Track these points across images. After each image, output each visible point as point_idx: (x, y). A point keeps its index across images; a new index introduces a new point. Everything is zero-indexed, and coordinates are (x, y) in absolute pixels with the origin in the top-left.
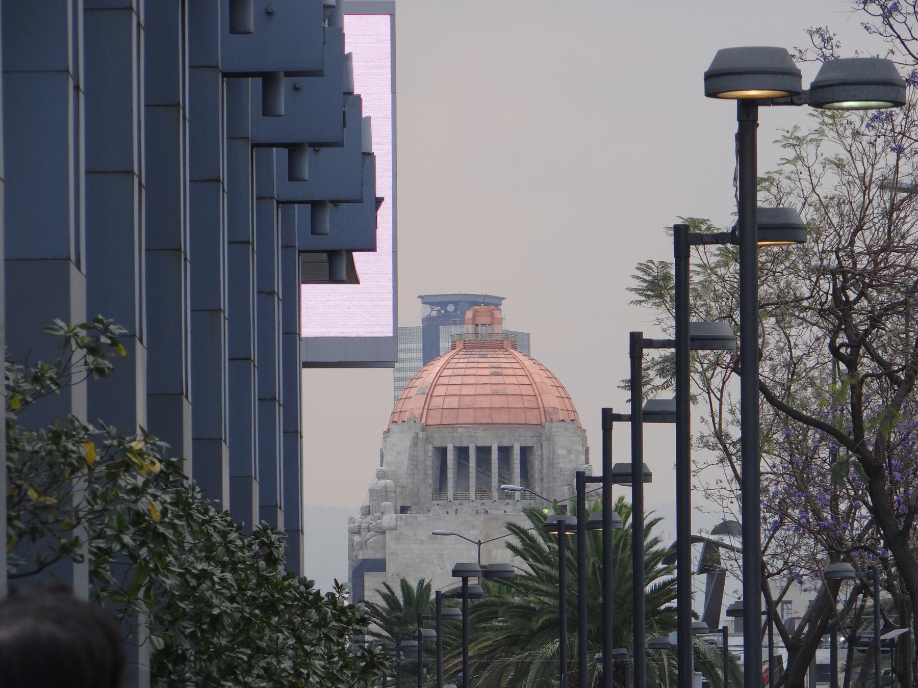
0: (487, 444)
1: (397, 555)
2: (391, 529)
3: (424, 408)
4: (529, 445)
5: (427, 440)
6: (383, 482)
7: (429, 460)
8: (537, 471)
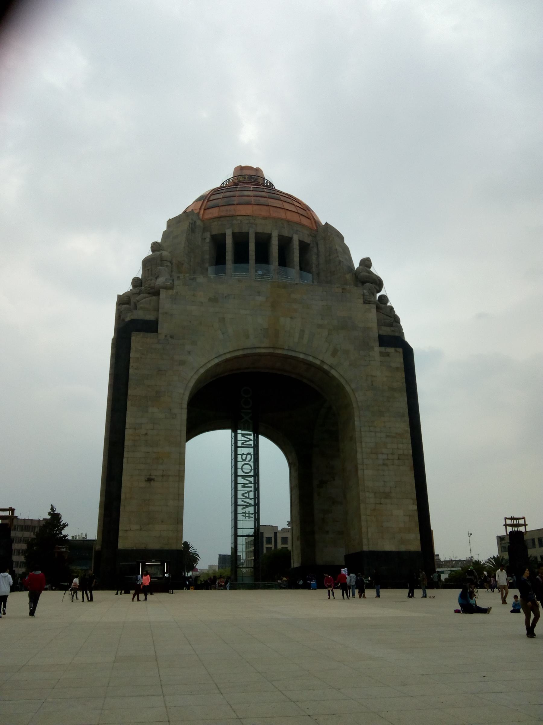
0: (267, 230)
2: (166, 288)
3: (200, 209)
4: (307, 240)
5: (205, 230)
6: (158, 253)
7: (207, 247)
8: (314, 265)
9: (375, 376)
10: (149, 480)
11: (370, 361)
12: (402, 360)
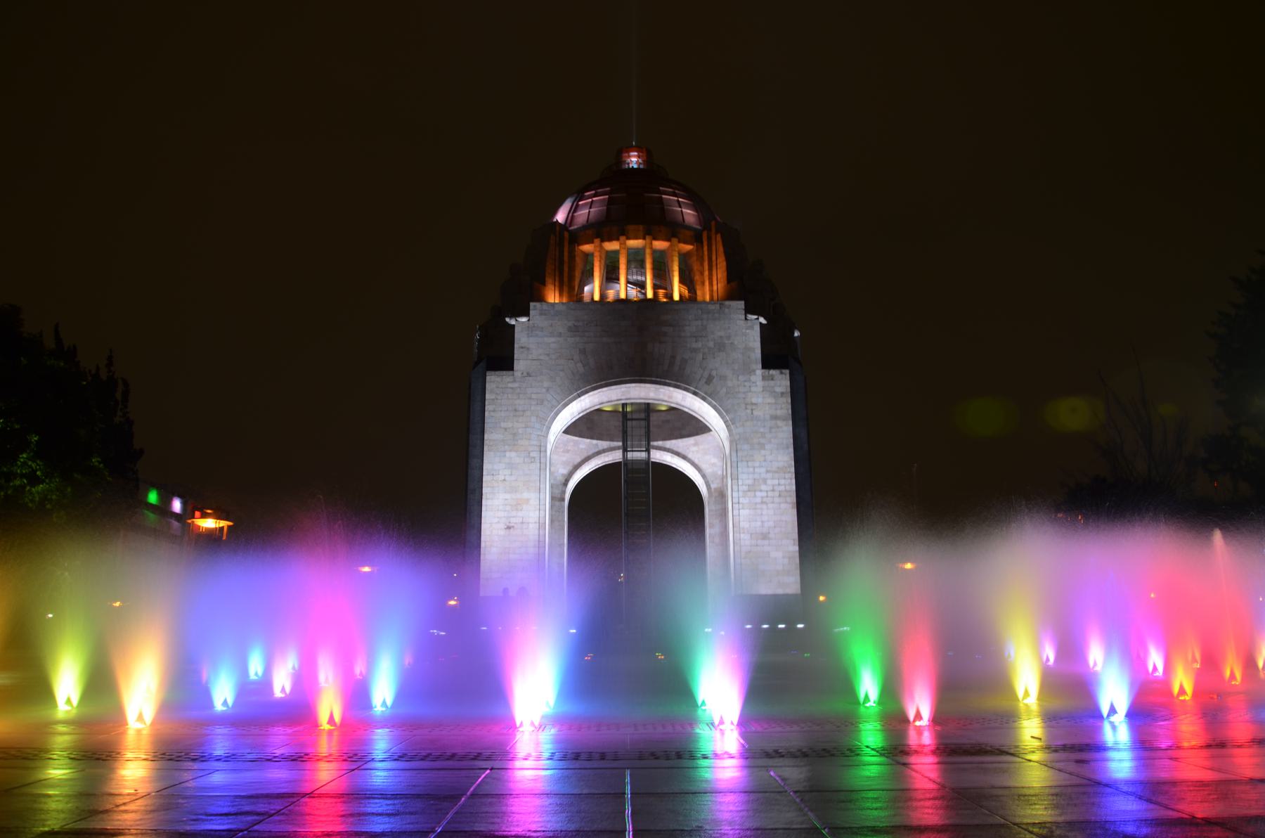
1: (528, 349)
9: (755, 404)
10: (509, 528)
11: (750, 387)
12: (788, 383)
